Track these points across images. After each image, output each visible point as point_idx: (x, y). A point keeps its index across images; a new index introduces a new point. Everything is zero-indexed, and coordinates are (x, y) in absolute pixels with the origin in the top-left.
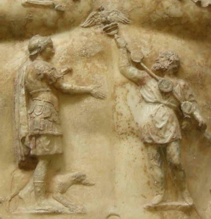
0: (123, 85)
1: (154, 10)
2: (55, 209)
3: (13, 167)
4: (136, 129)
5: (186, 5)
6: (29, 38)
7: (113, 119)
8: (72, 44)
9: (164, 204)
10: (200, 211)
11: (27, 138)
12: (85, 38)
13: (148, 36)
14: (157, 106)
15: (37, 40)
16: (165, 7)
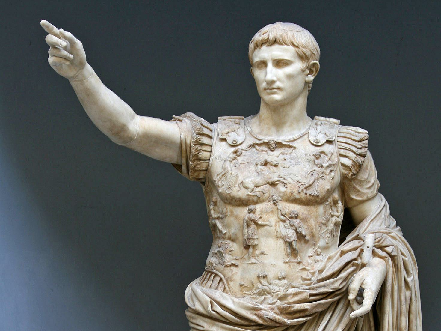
0: (278, 222)
1: (291, 196)
2: (255, 262)
3: (243, 248)
4: (282, 236)
5: (301, 195)
6: (249, 205)
7: (275, 233)
8: (262, 208)
9: (290, 261)
10: (304, 263)
11: (247, 239)
12: (267, 206)
13: (288, 205)
14: (289, 229)
15: (252, 207)
16: (294, 195)
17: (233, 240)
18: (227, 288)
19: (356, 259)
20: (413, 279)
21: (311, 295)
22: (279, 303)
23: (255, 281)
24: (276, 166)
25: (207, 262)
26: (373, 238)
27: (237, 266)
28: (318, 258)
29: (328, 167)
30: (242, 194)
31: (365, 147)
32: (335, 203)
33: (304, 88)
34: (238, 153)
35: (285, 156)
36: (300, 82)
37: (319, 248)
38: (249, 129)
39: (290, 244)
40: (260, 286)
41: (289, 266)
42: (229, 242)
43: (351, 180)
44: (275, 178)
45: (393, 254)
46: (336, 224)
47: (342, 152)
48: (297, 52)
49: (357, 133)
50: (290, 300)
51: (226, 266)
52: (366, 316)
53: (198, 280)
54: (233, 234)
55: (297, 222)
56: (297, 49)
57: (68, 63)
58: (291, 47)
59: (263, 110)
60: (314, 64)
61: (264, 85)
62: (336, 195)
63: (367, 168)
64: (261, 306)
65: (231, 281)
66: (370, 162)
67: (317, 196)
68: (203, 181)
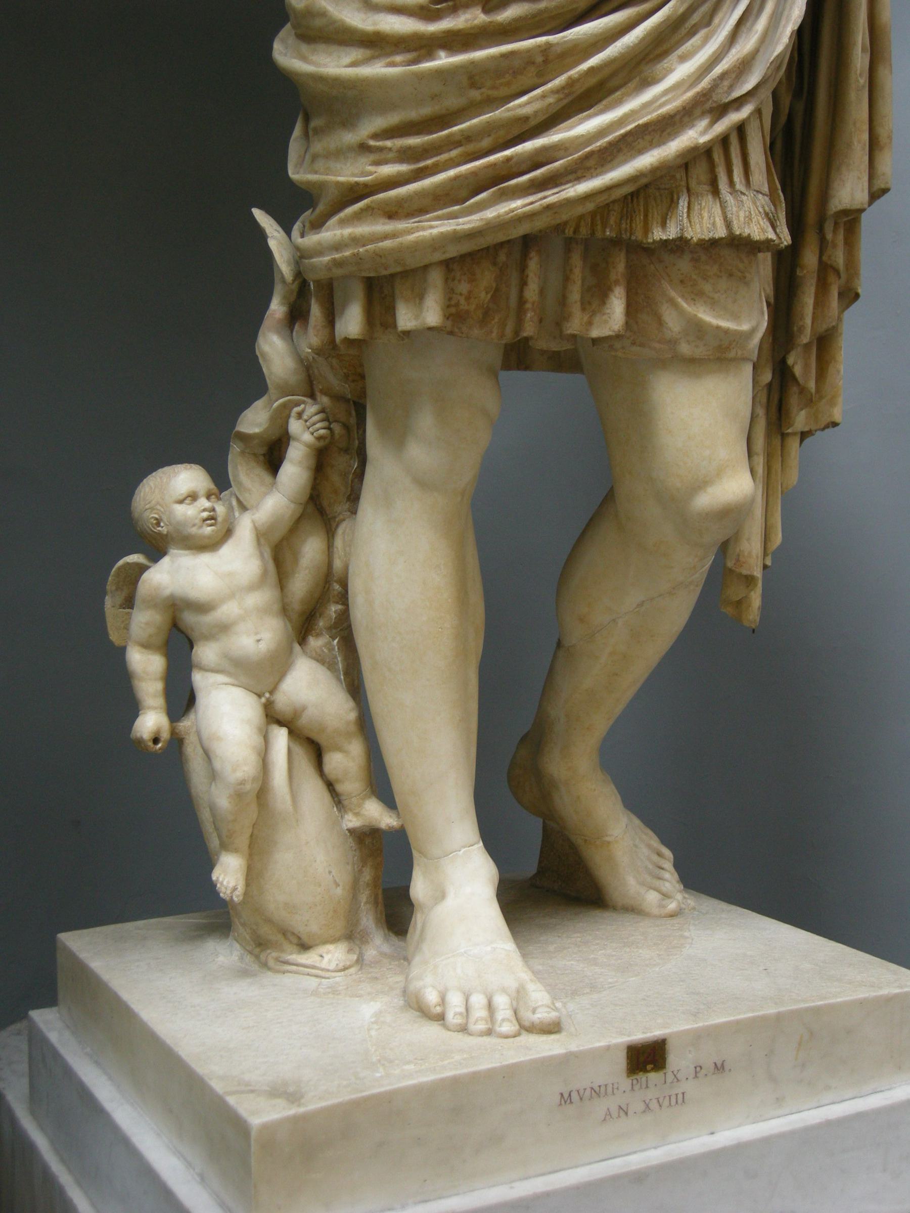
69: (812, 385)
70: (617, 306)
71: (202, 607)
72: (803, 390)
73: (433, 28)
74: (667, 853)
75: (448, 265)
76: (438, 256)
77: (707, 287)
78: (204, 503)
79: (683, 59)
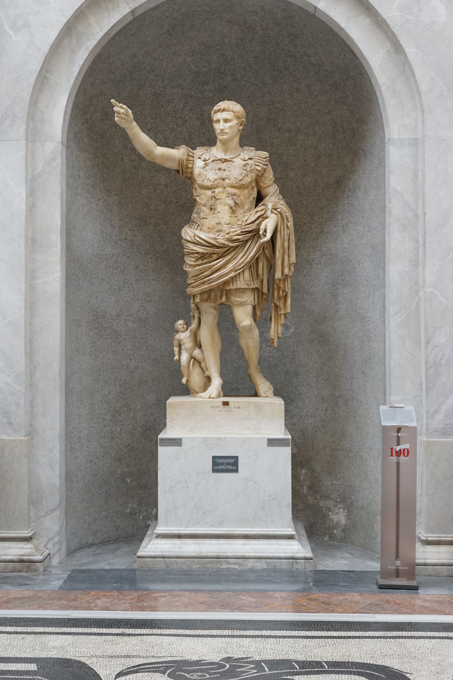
3: (209, 210)
15: (213, 190)
17: (205, 206)
18: (202, 229)
19: (263, 215)
20: (291, 224)
21: (242, 232)
22: (226, 236)
23: (215, 225)
24: (225, 170)
25: (192, 217)
26: (272, 205)
27: (206, 218)
28: (245, 214)
29: (250, 171)
30: (208, 184)
31: (267, 161)
32: (253, 188)
33: (238, 133)
34: (207, 165)
35: (229, 166)
36: (236, 130)
37: (245, 209)
38: (212, 153)
39: (232, 207)
40: (218, 228)
41: (231, 218)
42: (202, 207)
43: (260, 177)
44: (224, 176)
45: (281, 212)
46: (253, 198)
47: (256, 163)
48: (234, 115)
49: (263, 155)
50: (232, 234)
51: (201, 219)
52: (267, 242)
53: (188, 225)
54: (204, 203)
55: (235, 197)
56: (234, 114)
57: (125, 121)
58: (232, 113)
59: (218, 143)
60: (243, 121)
61: (219, 131)
62: (254, 184)
63: (268, 171)
64: (218, 237)
65: (204, 225)
66: (270, 169)
67: (244, 185)
68: (190, 178)
69: (282, 306)
70: (224, 299)
71: (182, 340)
72: (280, 308)
73: (195, 264)
74: (272, 389)
75: (200, 293)
76: (198, 293)
77: (237, 295)
78: (182, 325)
79: (231, 264)
